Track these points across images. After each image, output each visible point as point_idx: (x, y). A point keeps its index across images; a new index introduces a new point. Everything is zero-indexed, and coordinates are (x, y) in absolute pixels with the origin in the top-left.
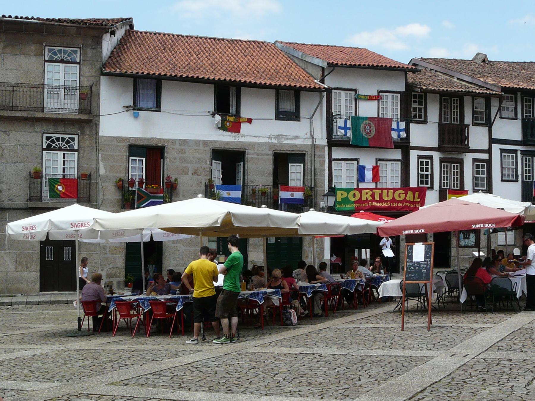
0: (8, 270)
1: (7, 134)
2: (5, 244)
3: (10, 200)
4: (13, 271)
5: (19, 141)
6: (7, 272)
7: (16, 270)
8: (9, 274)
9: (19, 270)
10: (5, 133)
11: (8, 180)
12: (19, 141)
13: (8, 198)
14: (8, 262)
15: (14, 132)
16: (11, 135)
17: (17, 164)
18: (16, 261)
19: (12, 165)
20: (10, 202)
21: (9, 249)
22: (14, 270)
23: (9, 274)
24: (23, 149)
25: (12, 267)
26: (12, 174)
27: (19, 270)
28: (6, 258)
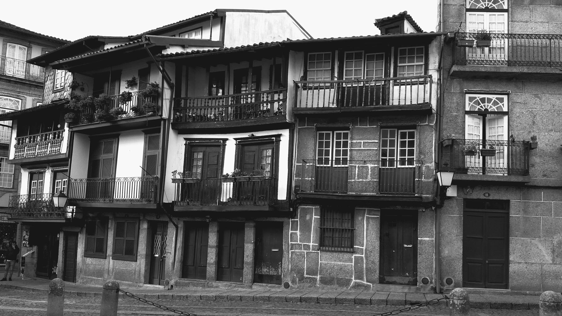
0: (544, 262)
1: (538, 97)
2: (539, 229)
3: (544, 176)
4: (550, 264)
5: (553, 105)
6: (542, 265)
7: (554, 263)
8: (544, 267)
9: (558, 263)
10: (536, 96)
11: (542, 152)
12: (553, 105)
13: (542, 174)
14: (544, 251)
15: (547, 95)
16: (543, 99)
17: (552, 133)
18: (553, 252)
19: (547, 133)
20: (545, 178)
21: (544, 236)
22: (551, 262)
23: (544, 267)
24: (559, 115)
25: (548, 258)
26: (546, 145)
27: (558, 263)
28: (540, 247)
